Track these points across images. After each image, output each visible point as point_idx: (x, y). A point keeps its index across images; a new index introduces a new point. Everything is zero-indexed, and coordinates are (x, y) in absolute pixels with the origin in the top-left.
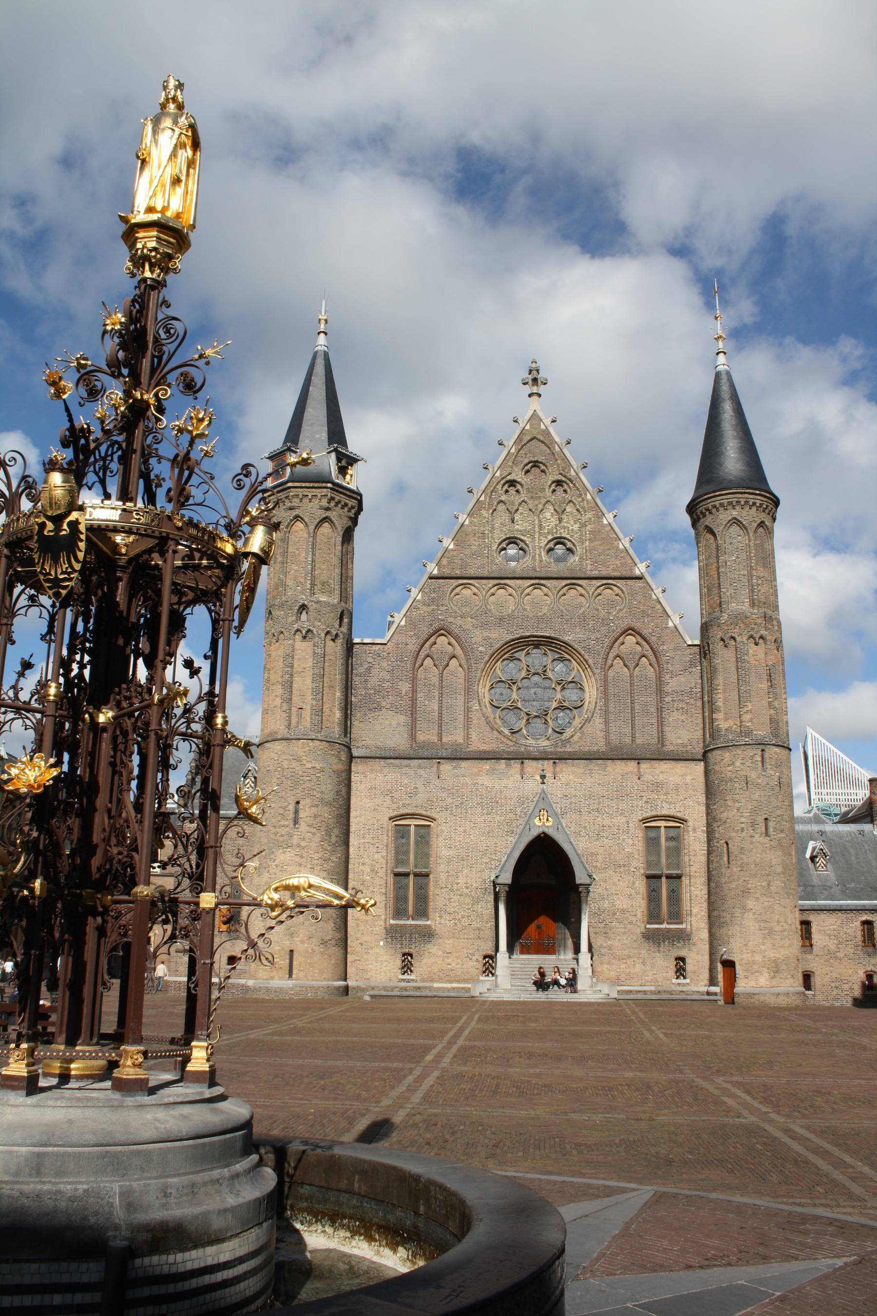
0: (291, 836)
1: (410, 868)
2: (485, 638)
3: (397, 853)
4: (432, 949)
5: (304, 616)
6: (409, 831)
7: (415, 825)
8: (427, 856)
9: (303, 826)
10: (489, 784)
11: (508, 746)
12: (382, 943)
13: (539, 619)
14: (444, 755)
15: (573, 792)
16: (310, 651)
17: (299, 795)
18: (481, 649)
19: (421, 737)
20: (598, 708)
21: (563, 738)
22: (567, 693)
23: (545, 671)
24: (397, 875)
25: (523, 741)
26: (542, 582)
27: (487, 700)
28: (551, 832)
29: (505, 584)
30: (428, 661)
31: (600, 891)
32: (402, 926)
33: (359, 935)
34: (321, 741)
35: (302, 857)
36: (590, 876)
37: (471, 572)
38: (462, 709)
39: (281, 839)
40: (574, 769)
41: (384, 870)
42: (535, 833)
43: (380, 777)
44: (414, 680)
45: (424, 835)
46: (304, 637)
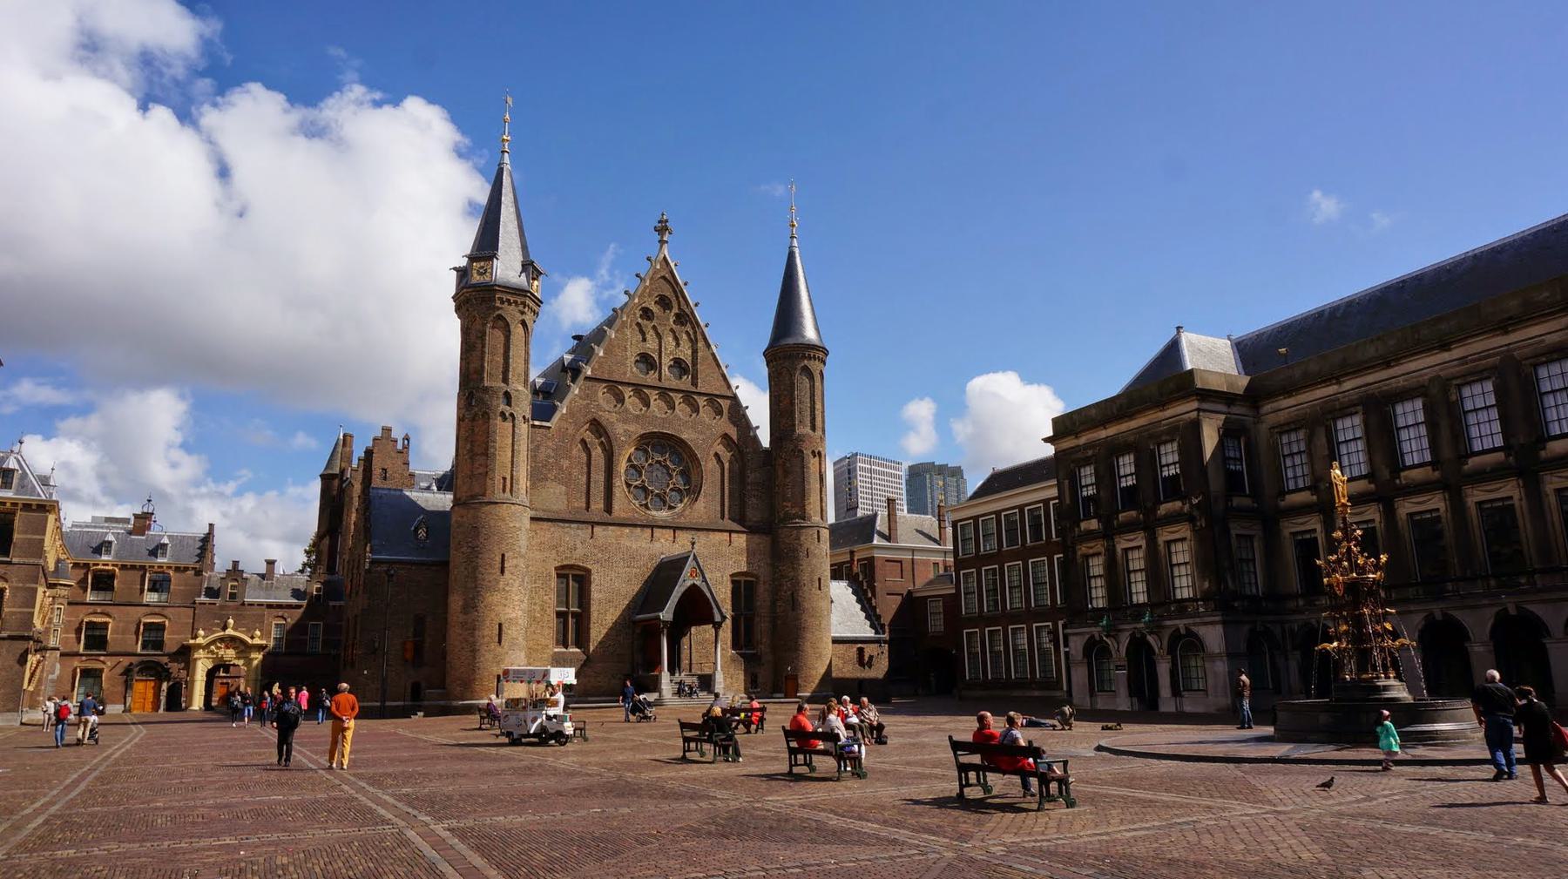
11: (641, 515)
42: (689, 583)
43: (548, 535)
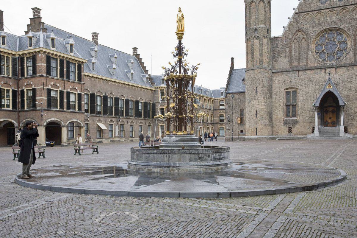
0: (255, 97)
1: (291, 103)
2: (312, 31)
3: (287, 99)
4: (297, 126)
5: (256, 32)
6: (290, 93)
7: (292, 91)
8: (296, 99)
9: (258, 94)
10: (314, 77)
12: (282, 125)
13: (332, 22)
14: (300, 69)
15: (342, 77)
16: (258, 42)
17: (257, 85)
18: (312, 34)
19: (293, 64)
20: (352, 49)
21: (340, 60)
22: (341, 45)
23: (334, 39)
24: (287, 106)
25: (326, 63)
26: (333, 9)
27: (314, 51)
28: (332, 90)
29: (320, 12)
30: (295, 41)
31: (350, 107)
32: (288, 120)
33: (276, 123)
34: (263, 69)
35: (258, 102)
36: (344, 103)
37: (309, 9)
38: (306, 54)
39: (253, 98)
40: (343, 70)
41: (283, 104)
42: (327, 91)
43: (281, 78)
44: (291, 48)
45: (295, 93)
46: (256, 39)
